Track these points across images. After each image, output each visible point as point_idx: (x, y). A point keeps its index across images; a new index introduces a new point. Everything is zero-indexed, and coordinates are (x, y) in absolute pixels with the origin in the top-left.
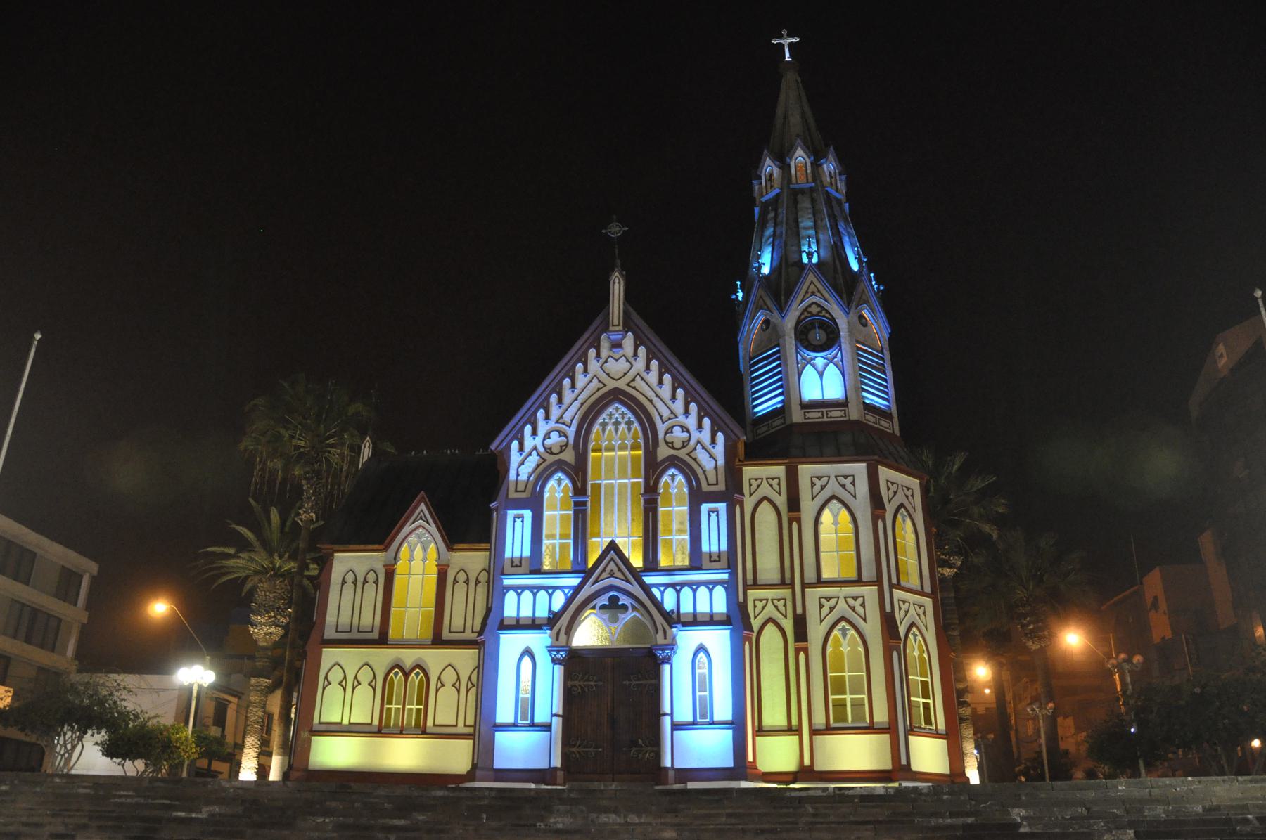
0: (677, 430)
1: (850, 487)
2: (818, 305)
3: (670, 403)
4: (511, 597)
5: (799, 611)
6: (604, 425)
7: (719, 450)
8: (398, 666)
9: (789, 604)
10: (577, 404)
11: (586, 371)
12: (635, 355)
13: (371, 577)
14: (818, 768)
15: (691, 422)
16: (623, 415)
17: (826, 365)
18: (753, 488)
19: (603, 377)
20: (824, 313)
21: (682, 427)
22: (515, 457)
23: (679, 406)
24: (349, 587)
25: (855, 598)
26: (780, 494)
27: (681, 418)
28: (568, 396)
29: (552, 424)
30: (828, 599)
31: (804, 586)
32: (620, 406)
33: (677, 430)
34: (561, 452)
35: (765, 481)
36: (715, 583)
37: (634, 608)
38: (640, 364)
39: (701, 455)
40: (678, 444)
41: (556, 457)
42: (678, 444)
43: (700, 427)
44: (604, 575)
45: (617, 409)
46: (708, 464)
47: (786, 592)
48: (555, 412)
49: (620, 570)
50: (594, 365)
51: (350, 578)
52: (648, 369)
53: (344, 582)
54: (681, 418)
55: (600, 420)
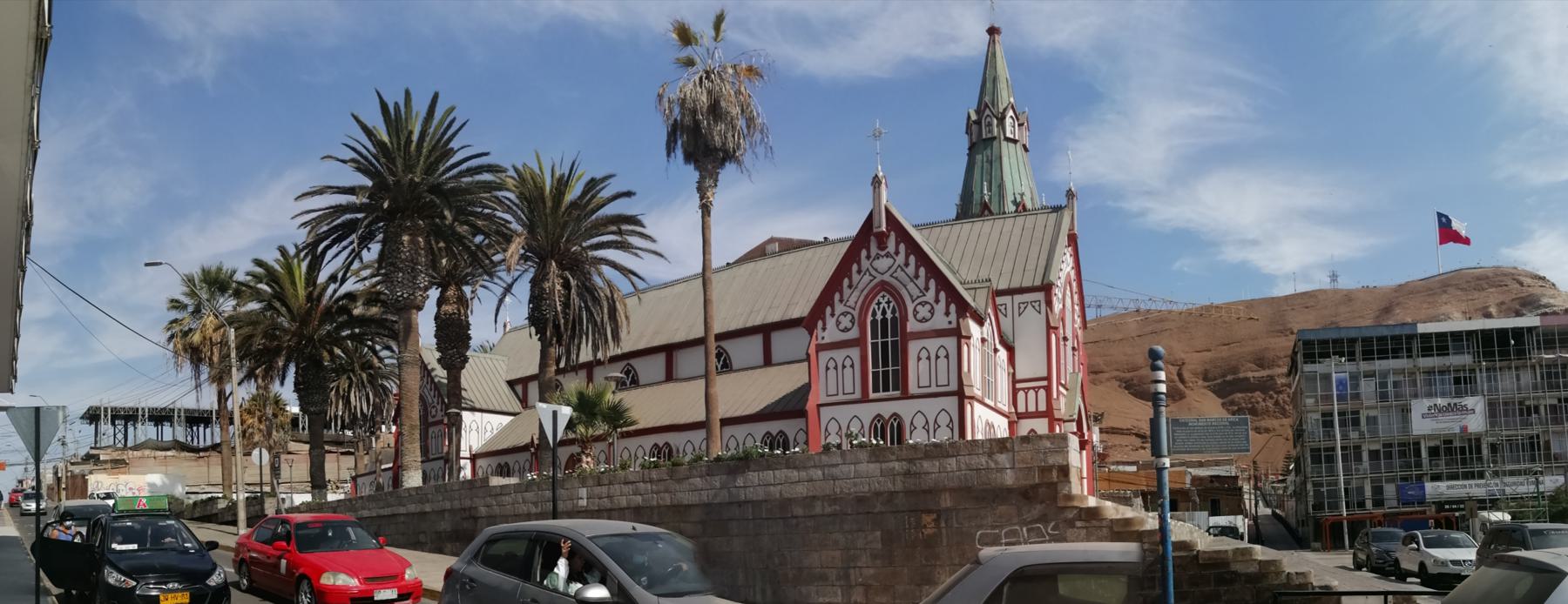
18: (1021, 310)
19: (874, 273)
35: (1029, 305)
45: (883, 297)
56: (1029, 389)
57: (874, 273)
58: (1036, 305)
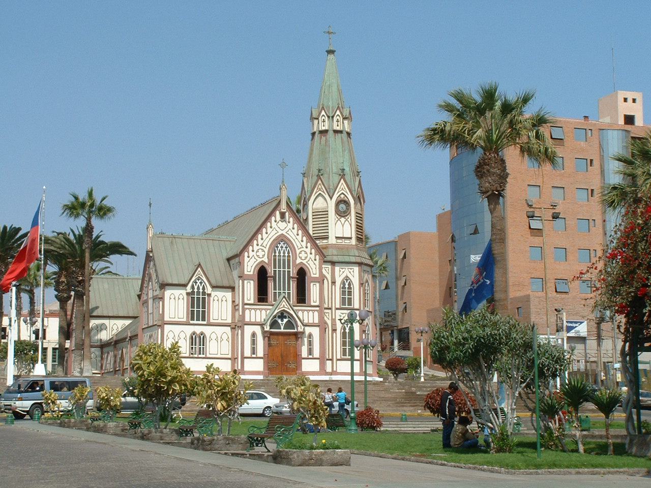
0: (303, 252)
1: (352, 273)
2: (344, 194)
3: (301, 243)
4: (247, 312)
5: (334, 317)
7: (317, 262)
8: (194, 333)
9: (330, 315)
10: (268, 239)
11: (271, 227)
13: (181, 297)
14: (338, 371)
15: (308, 250)
16: (284, 244)
17: (345, 221)
19: (278, 229)
20: (346, 198)
22: (246, 259)
23: (304, 244)
24: (172, 300)
26: (328, 274)
27: (304, 249)
29: (259, 247)
30: (343, 314)
33: (303, 252)
34: (263, 257)
37: (289, 317)
38: (290, 225)
39: (310, 262)
40: (303, 258)
41: (261, 260)
42: (303, 258)
43: (311, 254)
44: (282, 306)
46: (313, 266)
47: (330, 311)
48: (260, 242)
50: (274, 224)
51: (172, 297)
52: (293, 228)
53: (170, 298)
54: (304, 249)
56: (310, 310)
57: (278, 229)
58: (327, 269)
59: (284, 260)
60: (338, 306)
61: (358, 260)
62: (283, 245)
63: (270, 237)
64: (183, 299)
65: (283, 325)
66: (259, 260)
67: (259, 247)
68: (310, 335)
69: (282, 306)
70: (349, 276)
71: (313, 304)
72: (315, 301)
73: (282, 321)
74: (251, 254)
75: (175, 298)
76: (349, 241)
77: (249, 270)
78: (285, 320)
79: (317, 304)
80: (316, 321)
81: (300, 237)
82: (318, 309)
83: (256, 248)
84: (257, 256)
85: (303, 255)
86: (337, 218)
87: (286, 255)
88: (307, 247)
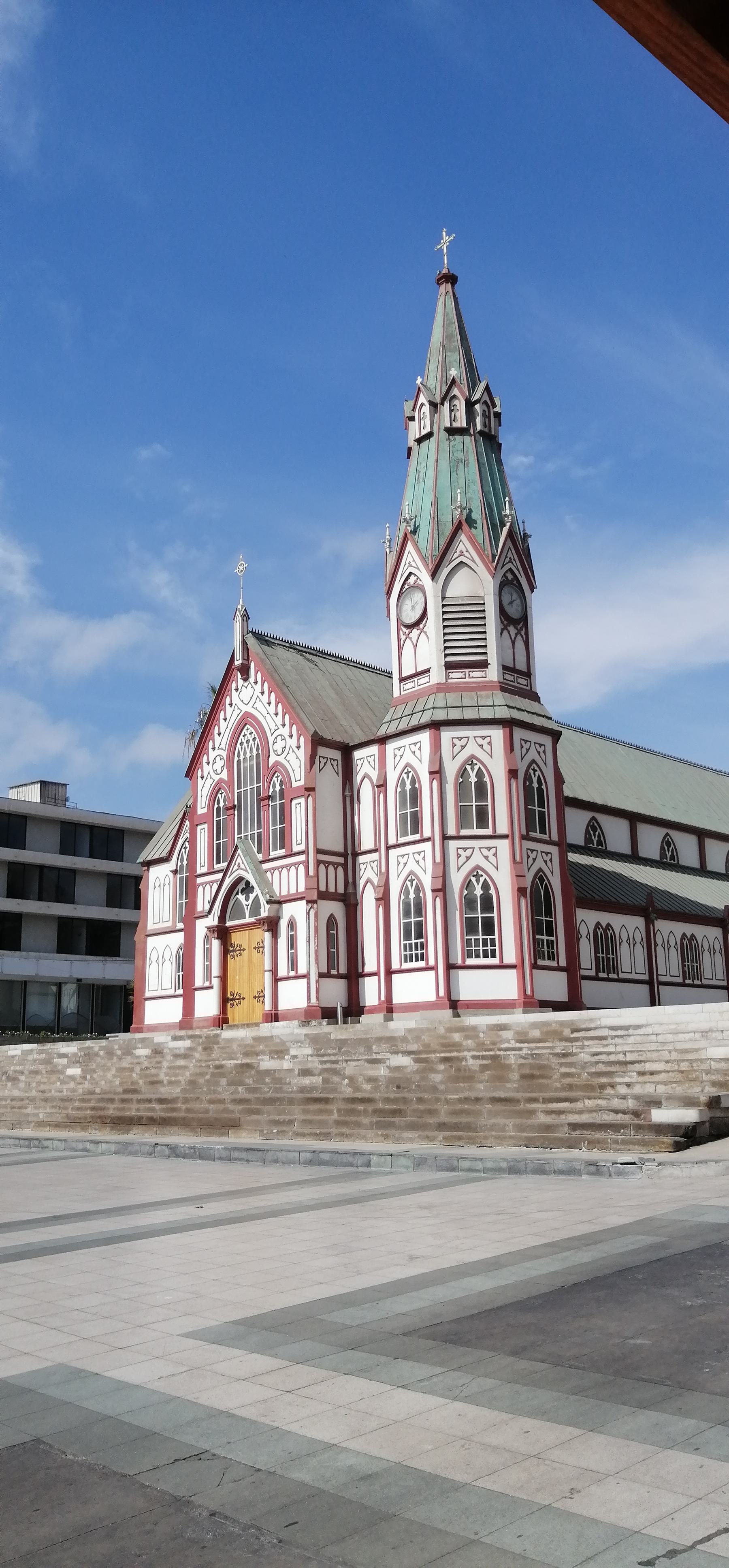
2: (415, 575)
6: (242, 744)
7: (301, 753)
10: (228, 730)
12: (256, 683)
15: (285, 731)
21: (281, 735)
24: (157, 889)
25: (419, 853)
28: (223, 725)
31: (388, 848)
32: (249, 727)
36: (299, 863)
38: (258, 688)
40: (280, 752)
42: (280, 752)
43: (291, 736)
44: (236, 867)
46: (295, 763)
47: (375, 856)
49: (243, 863)
51: (157, 885)
53: (155, 887)
55: (239, 741)
58: (371, 759)
59: (251, 767)
60: (392, 841)
61: (426, 718)
62: (250, 738)
63: (230, 727)
64: (169, 884)
65: (249, 907)
66: (217, 778)
67: (217, 752)
68: (292, 925)
69: (236, 867)
70: (415, 762)
71: (296, 849)
72: (299, 842)
73: (247, 899)
74: (207, 769)
75: (160, 886)
76: (426, 679)
77: (203, 806)
78: (252, 896)
79: (302, 847)
80: (302, 889)
81: (272, 709)
82: (302, 858)
83: (212, 754)
84: (214, 771)
85: (279, 746)
86: (404, 633)
87: (255, 753)
88: (284, 725)
